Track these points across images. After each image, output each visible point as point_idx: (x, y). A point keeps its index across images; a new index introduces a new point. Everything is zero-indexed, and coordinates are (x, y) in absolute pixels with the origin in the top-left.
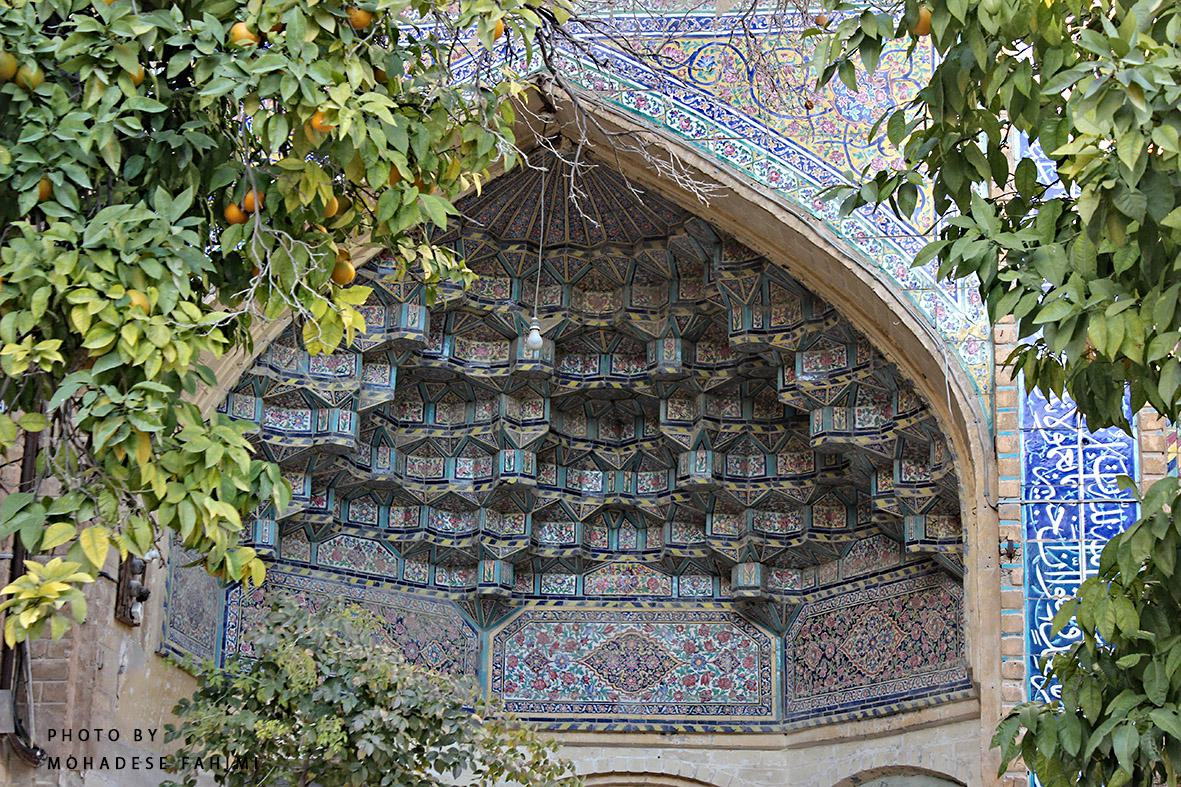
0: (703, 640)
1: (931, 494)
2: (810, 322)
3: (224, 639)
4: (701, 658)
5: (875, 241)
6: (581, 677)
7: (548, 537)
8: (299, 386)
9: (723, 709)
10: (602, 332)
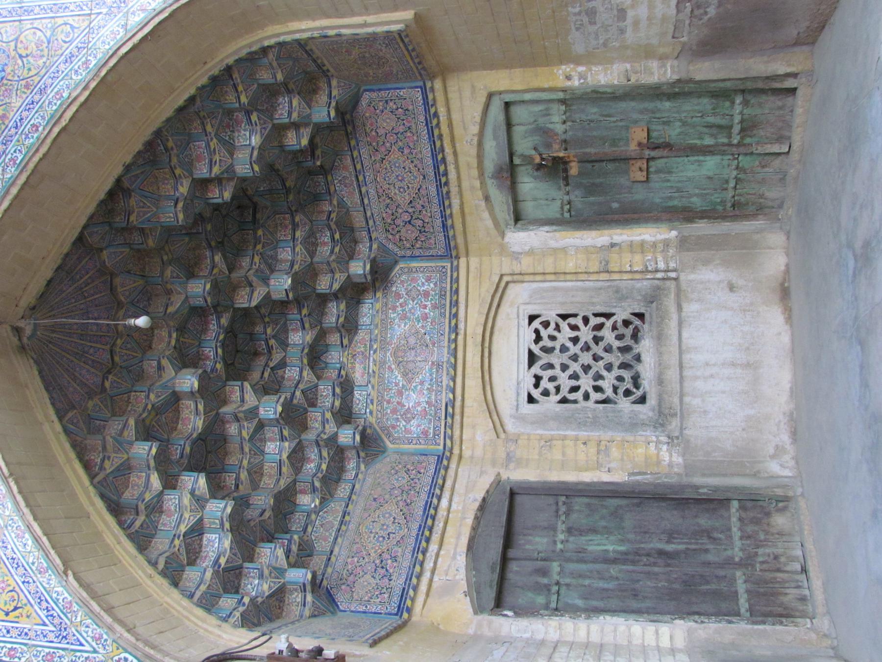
0: (399, 309)
1: (339, 247)
2: (170, 161)
3: (375, 613)
4: (410, 310)
5: (90, 55)
6: (420, 386)
7: (327, 404)
8: (181, 538)
9: (442, 296)
10: (182, 339)
